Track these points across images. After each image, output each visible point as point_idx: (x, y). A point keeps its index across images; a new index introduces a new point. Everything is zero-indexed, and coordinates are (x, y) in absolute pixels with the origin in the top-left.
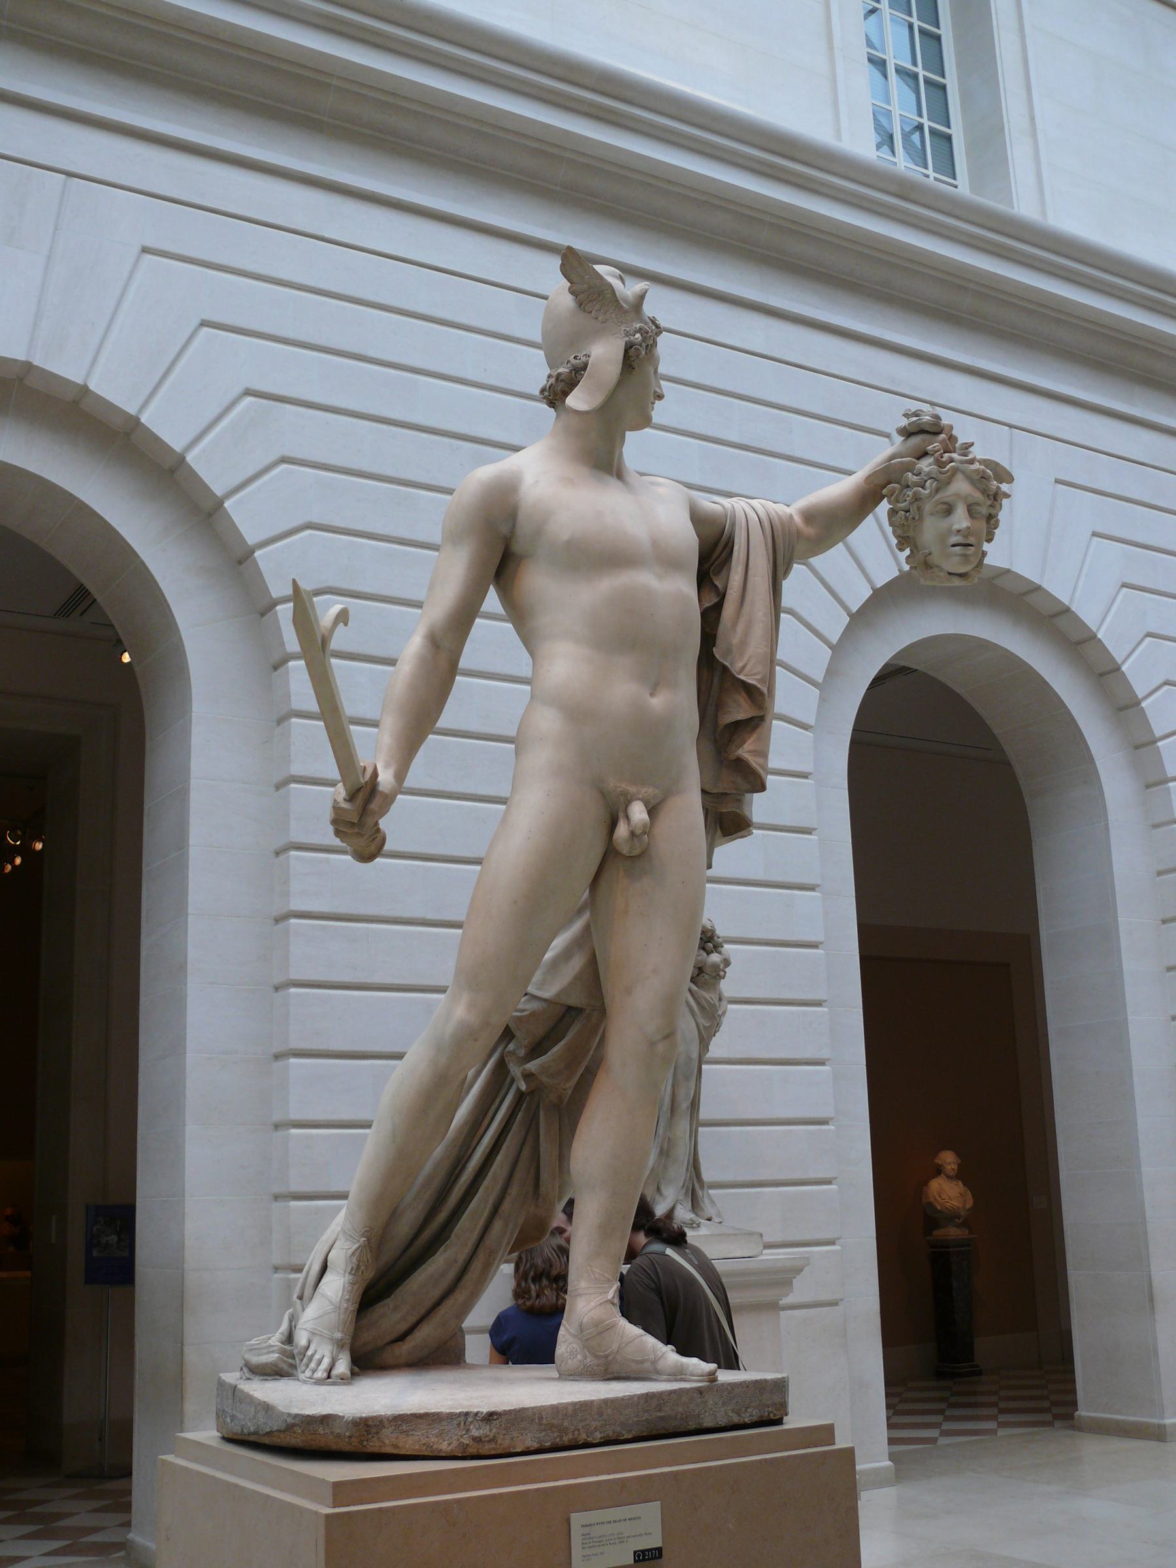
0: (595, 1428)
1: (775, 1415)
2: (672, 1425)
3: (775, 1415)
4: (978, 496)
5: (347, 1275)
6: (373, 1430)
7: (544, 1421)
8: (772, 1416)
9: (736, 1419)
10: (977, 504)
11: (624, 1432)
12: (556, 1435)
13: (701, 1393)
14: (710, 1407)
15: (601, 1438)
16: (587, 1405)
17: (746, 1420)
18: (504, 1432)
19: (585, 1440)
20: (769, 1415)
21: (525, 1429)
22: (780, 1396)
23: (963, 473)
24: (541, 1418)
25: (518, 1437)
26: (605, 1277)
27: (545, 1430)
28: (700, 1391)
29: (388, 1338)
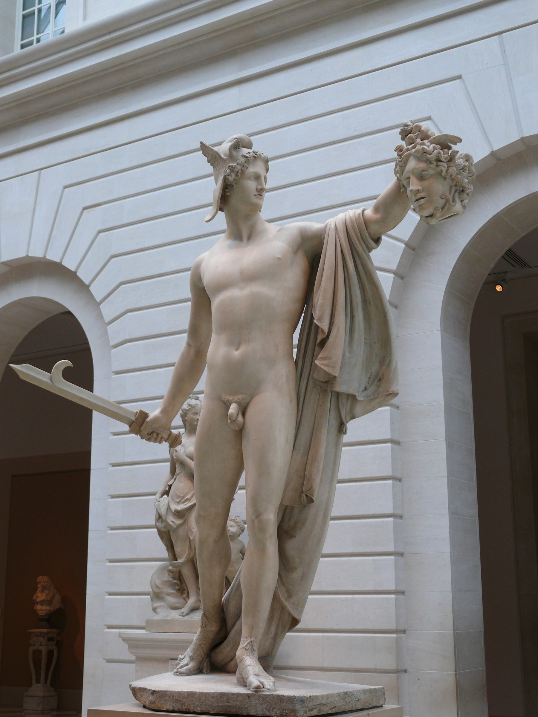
0: (198, 705)
4: (422, 165)
7: (175, 698)
10: (423, 171)
11: (210, 710)
12: (180, 705)
13: (249, 697)
17: (273, 715)
18: (158, 700)
20: (286, 715)
21: (167, 700)
23: (413, 155)
24: (173, 696)
25: (164, 703)
26: (245, 635)
27: (175, 702)
28: (248, 696)
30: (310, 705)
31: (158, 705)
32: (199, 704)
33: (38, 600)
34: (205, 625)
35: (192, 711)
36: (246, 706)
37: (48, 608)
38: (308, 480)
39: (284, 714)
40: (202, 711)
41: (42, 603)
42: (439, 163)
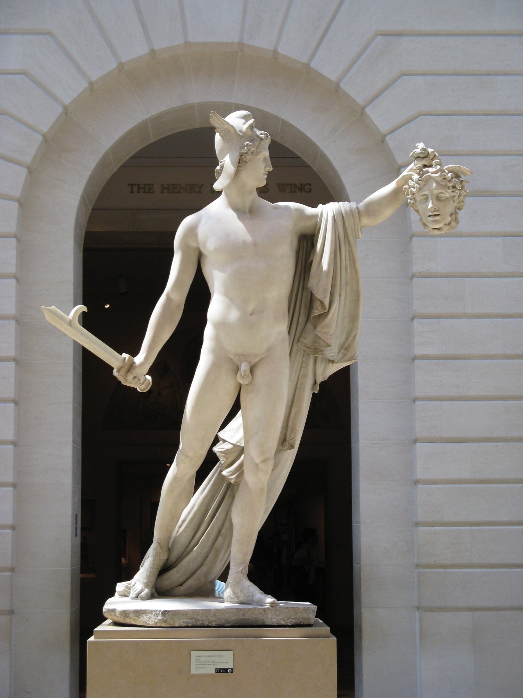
1: (303, 623)
5: (152, 557)
6: (128, 615)
7: (189, 616)
8: (302, 623)
12: (194, 621)
16: (208, 611)
19: (208, 624)
20: (300, 623)
22: (306, 615)
27: (188, 619)
28: (264, 610)
29: (176, 584)
34: (159, 554)
38: (292, 430)
40: (216, 624)
42: (455, 190)
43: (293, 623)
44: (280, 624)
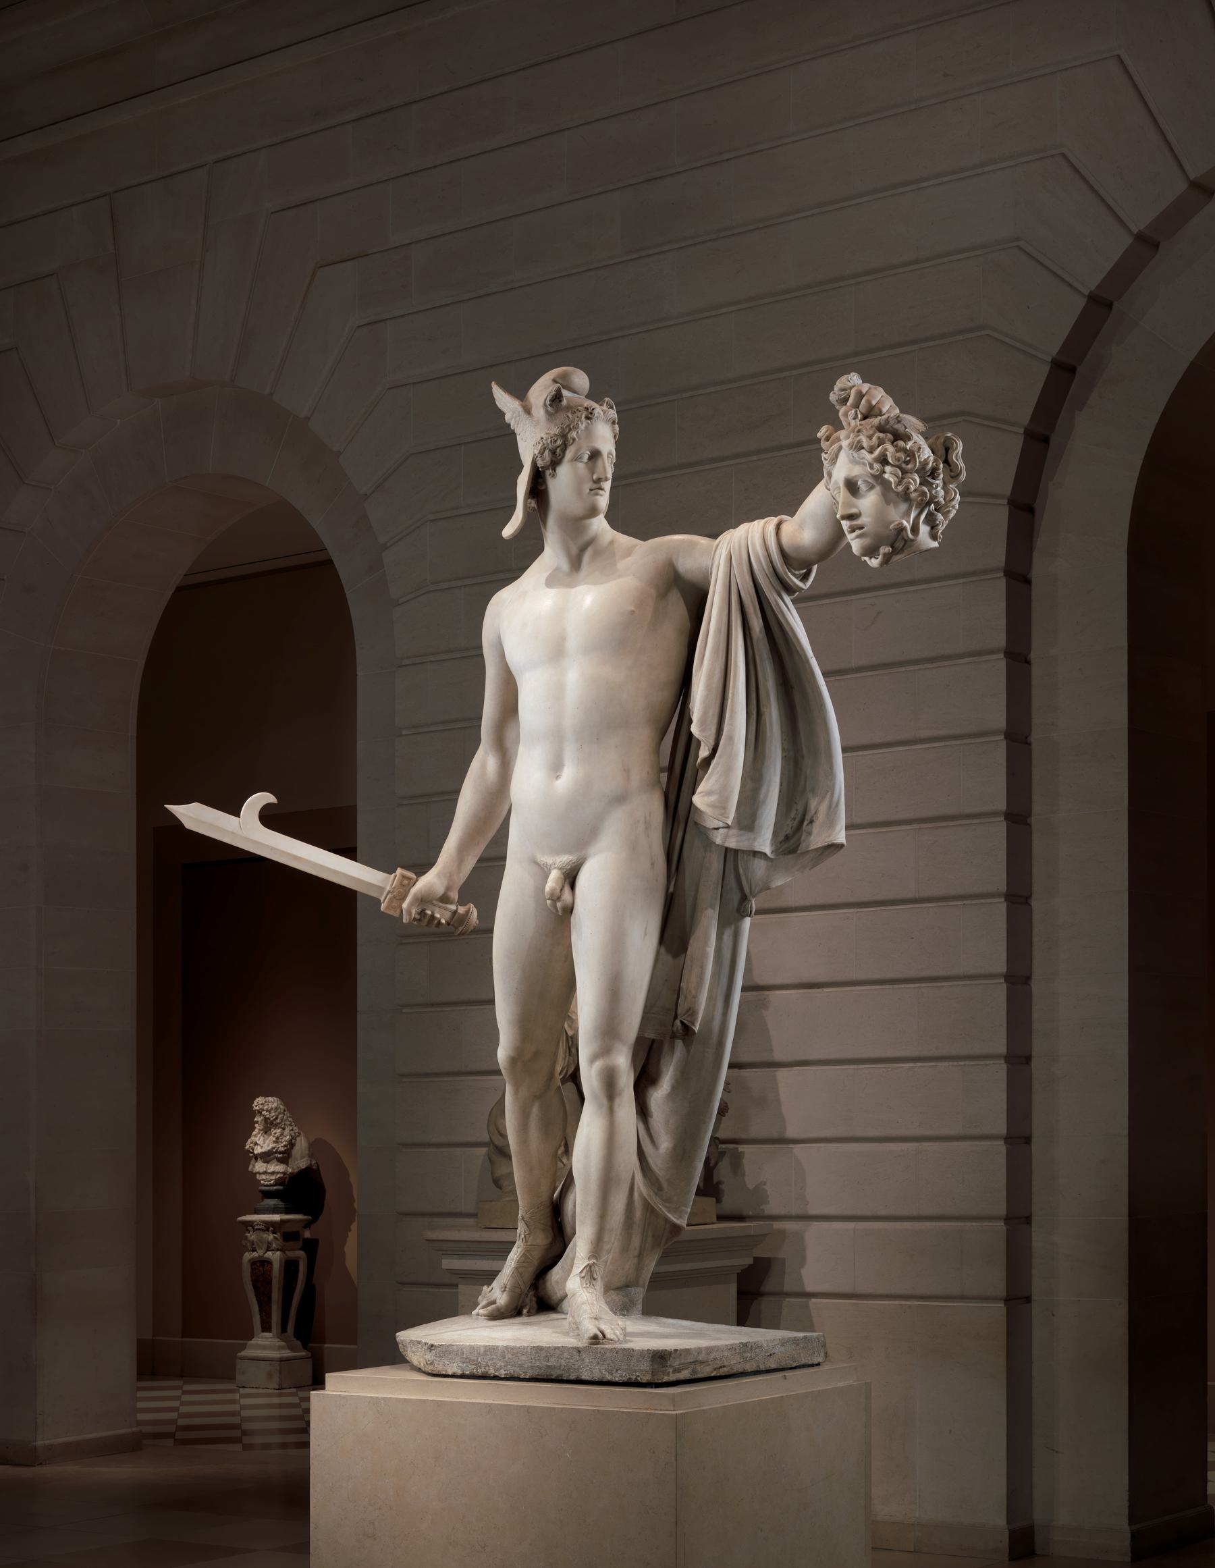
0: (501, 1366)
1: (641, 1379)
2: (555, 1374)
3: (641, 1379)
7: (465, 1356)
9: (609, 1377)
12: (473, 1367)
13: (579, 1351)
14: (587, 1364)
15: (505, 1374)
16: (494, 1349)
17: (617, 1379)
20: (636, 1379)
21: (453, 1360)
24: (462, 1353)
28: (579, 1350)
30: (676, 1363)
31: (439, 1367)
32: (503, 1364)
33: (258, 1150)
35: (492, 1375)
36: (576, 1367)
37: (280, 1168)
39: (634, 1377)
41: (267, 1157)
43: (624, 1378)
44: (605, 1380)
